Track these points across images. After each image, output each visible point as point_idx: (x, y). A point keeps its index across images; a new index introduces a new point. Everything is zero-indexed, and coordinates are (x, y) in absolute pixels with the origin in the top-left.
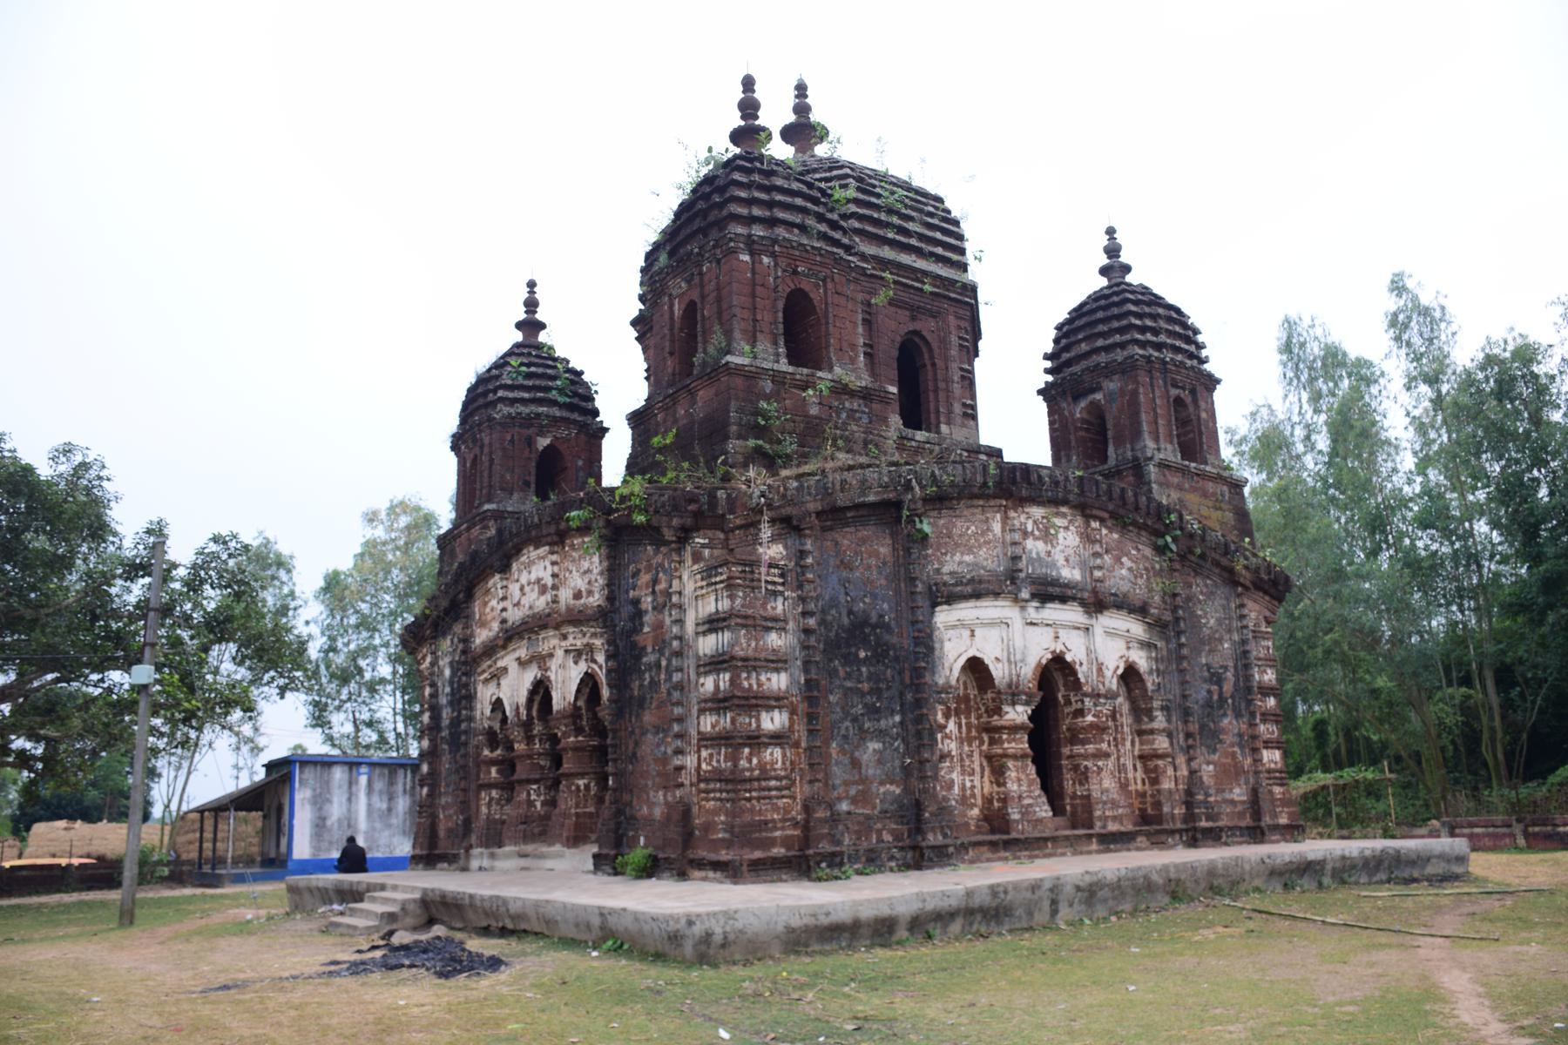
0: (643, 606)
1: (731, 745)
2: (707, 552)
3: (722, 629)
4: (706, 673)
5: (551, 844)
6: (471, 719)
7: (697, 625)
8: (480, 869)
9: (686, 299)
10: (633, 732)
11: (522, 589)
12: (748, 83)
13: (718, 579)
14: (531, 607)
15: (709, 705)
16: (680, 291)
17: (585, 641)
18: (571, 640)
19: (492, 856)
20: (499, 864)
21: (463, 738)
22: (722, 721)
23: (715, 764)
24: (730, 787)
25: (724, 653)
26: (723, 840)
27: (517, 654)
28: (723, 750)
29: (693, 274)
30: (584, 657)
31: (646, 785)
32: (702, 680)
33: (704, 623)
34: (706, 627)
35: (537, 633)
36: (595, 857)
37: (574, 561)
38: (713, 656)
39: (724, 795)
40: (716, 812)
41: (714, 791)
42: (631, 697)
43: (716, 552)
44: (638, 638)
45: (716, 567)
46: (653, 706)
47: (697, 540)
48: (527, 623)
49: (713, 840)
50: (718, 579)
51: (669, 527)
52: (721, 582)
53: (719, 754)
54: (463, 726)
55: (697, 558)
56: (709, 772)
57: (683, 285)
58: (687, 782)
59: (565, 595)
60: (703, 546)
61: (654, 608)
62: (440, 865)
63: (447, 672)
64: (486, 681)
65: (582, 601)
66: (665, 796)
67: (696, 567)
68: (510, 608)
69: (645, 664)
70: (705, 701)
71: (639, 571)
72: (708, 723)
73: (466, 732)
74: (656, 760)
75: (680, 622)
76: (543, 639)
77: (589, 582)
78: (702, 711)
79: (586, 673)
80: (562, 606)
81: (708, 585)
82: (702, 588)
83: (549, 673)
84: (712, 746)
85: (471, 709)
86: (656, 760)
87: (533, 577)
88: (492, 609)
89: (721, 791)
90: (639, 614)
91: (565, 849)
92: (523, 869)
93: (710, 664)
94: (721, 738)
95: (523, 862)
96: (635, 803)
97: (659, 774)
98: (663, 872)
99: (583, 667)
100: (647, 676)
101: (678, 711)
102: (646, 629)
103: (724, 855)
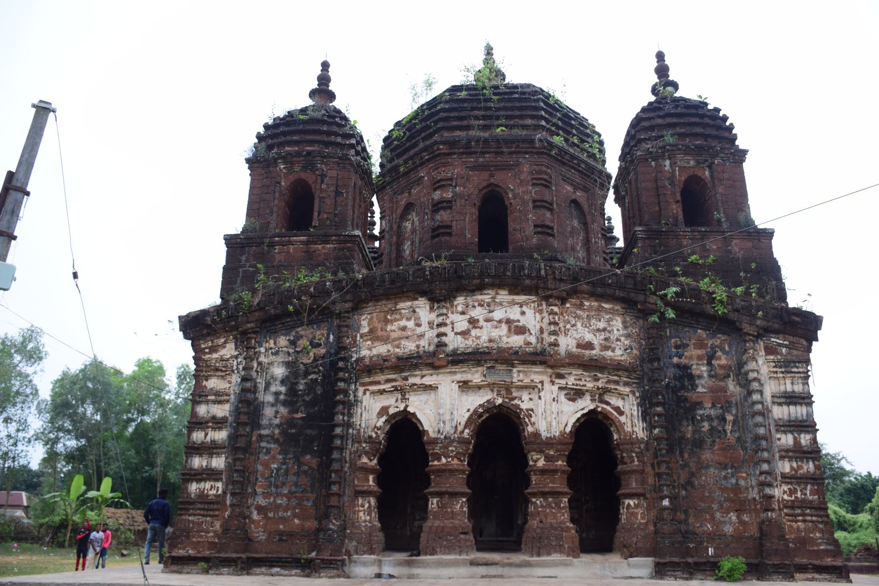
0: (695, 372)
1: (818, 484)
2: (784, 350)
3: (801, 404)
4: (785, 432)
5: (549, 554)
6: (349, 425)
7: (772, 397)
8: (379, 576)
9: (691, 172)
10: (686, 465)
11: (473, 322)
12: (660, 56)
13: (795, 370)
14: (490, 341)
15: (790, 454)
16: (685, 165)
17: (600, 384)
18: (571, 381)
19: (409, 564)
20: (416, 571)
21: (338, 442)
22: (805, 467)
23: (799, 494)
24: (818, 513)
25: (803, 421)
26: (826, 551)
27: (459, 377)
28: (809, 487)
29: (706, 161)
30: (588, 397)
31: (710, 508)
32: (778, 436)
33: (779, 397)
34: (783, 400)
35: (513, 366)
36: (657, 565)
37: (578, 317)
38: (790, 421)
39: (814, 518)
40: (807, 530)
41: (803, 515)
42: (683, 438)
43: (795, 352)
44: (692, 396)
45: (794, 362)
46: (716, 447)
47: (772, 339)
48: (489, 353)
49: (810, 551)
50: (795, 370)
51: (751, 324)
52: (798, 373)
53: (805, 489)
54: (338, 430)
55: (769, 350)
56: (793, 501)
57: (692, 163)
58: (777, 508)
59: (567, 343)
60: (780, 345)
61: (710, 376)
62: (257, 570)
63: (279, 371)
64: (382, 392)
65: (594, 352)
66: (738, 517)
67: (772, 357)
68: (451, 335)
69: (701, 416)
70: (787, 451)
71: (688, 345)
72: (785, 467)
73: (342, 437)
74: (723, 489)
75: (761, 392)
76: (519, 372)
77: (606, 339)
78: (782, 458)
79: (593, 412)
80: (562, 350)
81: (782, 372)
82: (776, 372)
83: (516, 402)
84: (798, 484)
85: (350, 415)
86: (723, 489)
87: (498, 314)
88: (404, 329)
89: (812, 516)
90: (686, 375)
91: (571, 558)
92: (483, 577)
93: (789, 426)
94: (807, 478)
95: (482, 570)
96: (691, 520)
97: (728, 500)
98: (770, 575)
99: (586, 404)
100: (706, 425)
101: (766, 455)
102: (700, 389)
103: (829, 561)
